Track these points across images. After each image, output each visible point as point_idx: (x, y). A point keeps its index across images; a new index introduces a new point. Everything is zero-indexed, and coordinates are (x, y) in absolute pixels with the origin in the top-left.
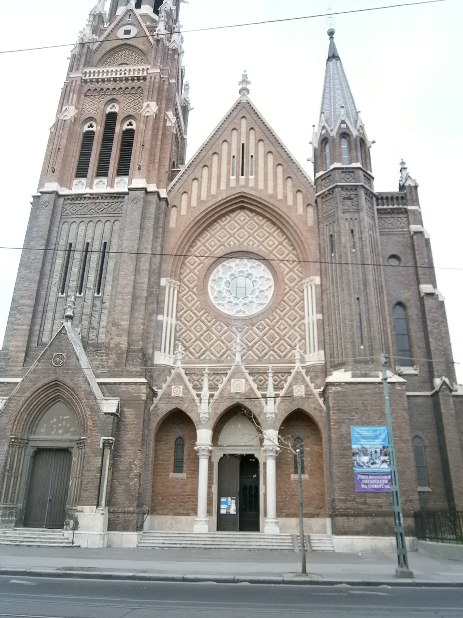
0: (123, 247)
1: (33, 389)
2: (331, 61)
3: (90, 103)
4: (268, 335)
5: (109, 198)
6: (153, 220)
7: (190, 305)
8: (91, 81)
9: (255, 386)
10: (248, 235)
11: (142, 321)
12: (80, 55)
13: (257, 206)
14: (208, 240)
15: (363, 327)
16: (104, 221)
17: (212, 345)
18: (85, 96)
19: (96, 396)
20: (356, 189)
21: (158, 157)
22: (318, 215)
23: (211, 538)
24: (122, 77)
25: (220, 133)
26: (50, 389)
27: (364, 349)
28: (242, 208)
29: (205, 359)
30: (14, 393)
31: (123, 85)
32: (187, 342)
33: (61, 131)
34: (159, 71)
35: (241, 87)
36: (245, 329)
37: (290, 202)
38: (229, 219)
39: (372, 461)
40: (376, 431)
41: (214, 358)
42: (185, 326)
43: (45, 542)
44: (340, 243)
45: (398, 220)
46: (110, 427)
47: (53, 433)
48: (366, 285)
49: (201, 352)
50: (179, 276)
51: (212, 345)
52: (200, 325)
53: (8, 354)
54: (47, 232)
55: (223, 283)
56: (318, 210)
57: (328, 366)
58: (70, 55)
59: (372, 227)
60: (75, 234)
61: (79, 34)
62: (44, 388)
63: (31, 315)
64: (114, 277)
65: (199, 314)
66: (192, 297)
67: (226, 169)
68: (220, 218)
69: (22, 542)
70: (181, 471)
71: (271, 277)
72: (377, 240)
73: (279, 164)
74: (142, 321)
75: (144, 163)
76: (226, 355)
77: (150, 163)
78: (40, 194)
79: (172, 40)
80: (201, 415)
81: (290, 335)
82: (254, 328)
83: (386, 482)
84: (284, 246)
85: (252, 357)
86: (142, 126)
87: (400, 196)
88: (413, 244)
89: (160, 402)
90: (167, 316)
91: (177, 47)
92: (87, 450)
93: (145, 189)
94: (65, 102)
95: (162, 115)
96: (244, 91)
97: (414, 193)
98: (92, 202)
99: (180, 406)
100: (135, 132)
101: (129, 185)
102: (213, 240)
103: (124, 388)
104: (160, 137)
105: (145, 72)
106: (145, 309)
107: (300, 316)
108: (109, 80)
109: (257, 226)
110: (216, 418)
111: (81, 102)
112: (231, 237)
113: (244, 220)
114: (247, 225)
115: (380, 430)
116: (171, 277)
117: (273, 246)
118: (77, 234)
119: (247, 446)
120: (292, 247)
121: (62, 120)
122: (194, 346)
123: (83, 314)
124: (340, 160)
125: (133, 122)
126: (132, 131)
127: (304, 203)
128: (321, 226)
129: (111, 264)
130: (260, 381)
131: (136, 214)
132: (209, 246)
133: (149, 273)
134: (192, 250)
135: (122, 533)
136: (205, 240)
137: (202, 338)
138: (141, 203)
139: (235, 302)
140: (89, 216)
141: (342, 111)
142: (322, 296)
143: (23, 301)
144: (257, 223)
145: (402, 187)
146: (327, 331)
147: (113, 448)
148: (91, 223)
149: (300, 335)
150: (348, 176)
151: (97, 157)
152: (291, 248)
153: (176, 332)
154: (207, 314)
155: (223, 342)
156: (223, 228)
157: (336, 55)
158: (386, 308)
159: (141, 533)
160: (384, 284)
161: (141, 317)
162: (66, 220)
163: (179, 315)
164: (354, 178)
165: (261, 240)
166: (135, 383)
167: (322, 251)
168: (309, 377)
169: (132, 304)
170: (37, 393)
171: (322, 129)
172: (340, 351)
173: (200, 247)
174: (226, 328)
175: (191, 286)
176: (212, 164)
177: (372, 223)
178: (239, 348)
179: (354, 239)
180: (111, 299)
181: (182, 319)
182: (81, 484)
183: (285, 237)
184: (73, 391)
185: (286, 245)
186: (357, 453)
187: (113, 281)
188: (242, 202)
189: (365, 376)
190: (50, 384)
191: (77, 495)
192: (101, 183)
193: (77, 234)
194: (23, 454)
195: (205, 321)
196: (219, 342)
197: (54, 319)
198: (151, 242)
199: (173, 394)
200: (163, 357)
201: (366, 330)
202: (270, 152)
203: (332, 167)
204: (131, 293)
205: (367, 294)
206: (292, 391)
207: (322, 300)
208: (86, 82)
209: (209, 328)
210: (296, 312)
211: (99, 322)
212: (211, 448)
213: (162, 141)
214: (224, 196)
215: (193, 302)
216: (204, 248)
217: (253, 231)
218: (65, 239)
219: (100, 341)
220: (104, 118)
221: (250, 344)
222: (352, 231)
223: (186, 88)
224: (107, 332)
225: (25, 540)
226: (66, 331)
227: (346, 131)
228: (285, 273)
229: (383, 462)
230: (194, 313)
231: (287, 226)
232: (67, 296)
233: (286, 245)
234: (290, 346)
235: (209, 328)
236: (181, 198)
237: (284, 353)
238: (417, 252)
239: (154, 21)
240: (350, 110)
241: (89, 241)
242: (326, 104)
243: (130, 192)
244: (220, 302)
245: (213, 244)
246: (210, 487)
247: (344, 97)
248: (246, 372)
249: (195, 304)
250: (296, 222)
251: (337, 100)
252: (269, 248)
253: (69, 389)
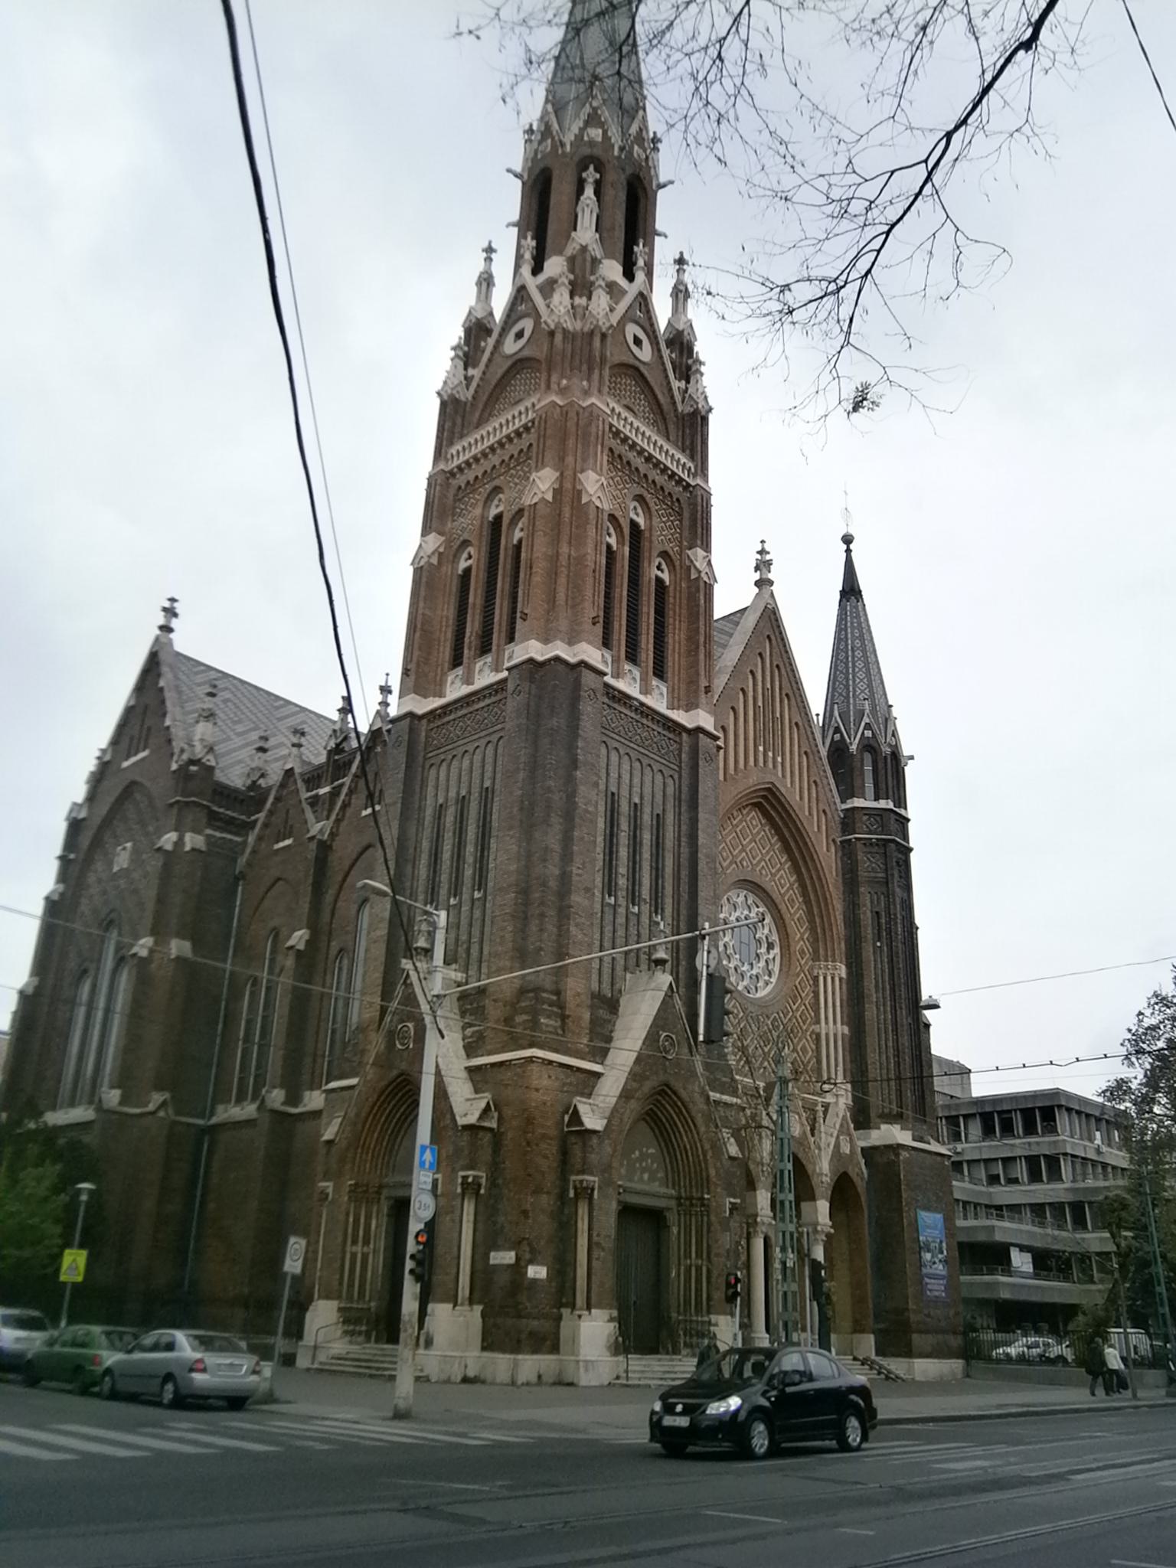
31: (661, 480)
118: (619, 776)
140: (635, 747)
188: (764, 797)
189: (921, 1140)
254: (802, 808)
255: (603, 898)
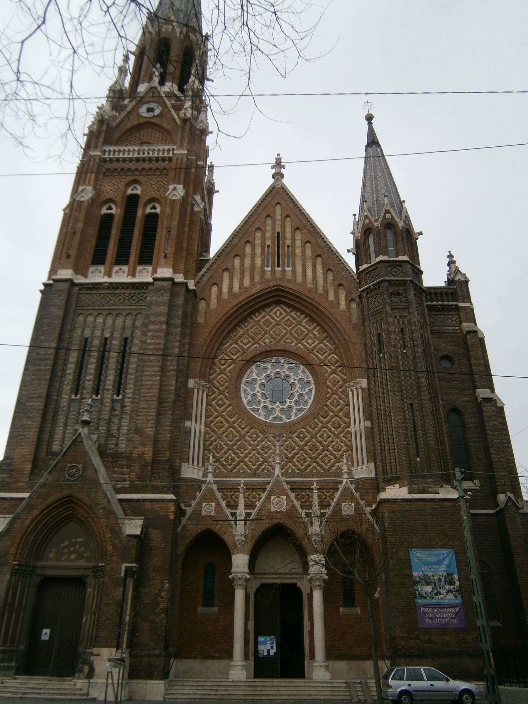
0: (148, 343)
1: (42, 506)
2: (371, 147)
3: (109, 184)
4: (309, 444)
5: (130, 288)
6: (180, 315)
7: (220, 410)
8: (111, 160)
9: (297, 504)
10: (285, 332)
11: (168, 428)
12: (99, 131)
13: (295, 301)
14: (240, 337)
15: (418, 437)
16: (124, 314)
17: (246, 456)
18: (104, 175)
19: (118, 515)
20: (404, 284)
21: (185, 244)
22: (363, 311)
23: (250, 686)
24: (145, 158)
25: (253, 220)
26: (62, 507)
27: (420, 462)
28: (278, 303)
29: (238, 472)
30: (19, 510)
31: (146, 165)
32: (218, 453)
33: (77, 213)
34: (185, 152)
35: (274, 171)
36: (284, 438)
37: (332, 297)
38: (264, 314)
39: (436, 591)
40: (439, 555)
41: (249, 471)
42: (216, 433)
43: (54, 694)
44: (390, 343)
45: (448, 318)
46: (133, 552)
47: (63, 559)
48: (420, 390)
49: (234, 464)
50: (208, 377)
51: (246, 456)
52: (233, 433)
53: (10, 465)
54: (60, 325)
55: (257, 386)
56: (362, 306)
57: (381, 481)
58: (87, 131)
59: (423, 326)
60: (91, 328)
61: (97, 110)
62: (55, 505)
63: (39, 419)
64: (136, 378)
65: (231, 421)
66: (223, 400)
67: (260, 260)
68: (253, 313)
69: (25, 693)
70: (212, 605)
71: (311, 379)
72: (429, 339)
73: (318, 256)
74: (168, 428)
75: (170, 251)
76: (263, 467)
77: (177, 251)
78: (51, 282)
79: (200, 120)
80: (237, 538)
81: (335, 445)
82: (294, 436)
83: (453, 615)
84: (325, 345)
85: (292, 469)
86: (168, 210)
87: (449, 292)
88: (466, 344)
89: (189, 522)
90: (196, 423)
91: (204, 127)
92: (106, 579)
93: (171, 280)
94: (82, 182)
95: (190, 199)
96: (278, 176)
97: (464, 289)
98: (111, 292)
99: (211, 527)
100: (160, 216)
101: (152, 275)
102: (246, 337)
103: (148, 506)
104: (187, 223)
105: (171, 153)
106: (173, 414)
107: (345, 423)
108: (131, 160)
109: (295, 323)
110: (254, 541)
111: (100, 182)
112: (265, 334)
113: (280, 315)
114: (283, 321)
115: (444, 554)
116: (199, 378)
117: (313, 345)
118: (94, 327)
119: (292, 574)
120: (334, 346)
121: (78, 201)
122: (225, 456)
123: (100, 419)
124: (386, 253)
125: (157, 205)
126: (156, 214)
127: (346, 297)
128: (367, 323)
129: (133, 362)
130: (303, 497)
131: (162, 307)
132: (241, 344)
133: (177, 373)
134: (223, 348)
135: (145, 681)
136: (237, 337)
137: (235, 448)
138: (168, 295)
139: (271, 407)
141: (386, 200)
142: (370, 400)
143: (30, 403)
144: (294, 319)
145: (450, 282)
146: (377, 441)
147: (136, 577)
148: (110, 316)
149: (346, 445)
150: (395, 270)
151: (117, 242)
152: (332, 348)
153: (205, 440)
154: (240, 420)
155: (259, 453)
156: (257, 323)
157: (376, 141)
158: (442, 415)
159: (168, 681)
160: (438, 388)
161: (168, 423)
162: (81, 312)
163: (208, 421)
164: (402, 272)
165: (299, 338)
166: (162, 500)
167: (369, 352)
168: (359, 493)
169: (158, 409)
170: (46, 511)
171: (365, 219)
172: (393, 464)
173: (232, 344)
174: (262, 436)
175: (222, 388)
176: (244, 253)
177: (422, 321)
178: (278, 458)
179: (403, 337)
180: (132, 402)
181: (212, 425)
182: (98, 621)
183: (325, 334)
184: (89, 508)
185: (327, 343)
186: (419, 582)
187: (135, 382)
188: (279, 295)
190: (63, 500)
191: (92, 634)
192: (121, 272)
193: (94, 327)
194: (27, 585)
195: (238, 428)
196: (254, 452)
197: (66, 425)
198: (179, 339)
199: (204, 513)
200: (191, 469)
201: (421, 439)
202: (308, 242)
203: (378, 260)
204: (157, 396)
205: (421, 400)
206: (340, 509)
207: (371, 406)
208: (105, 160)
209: (242, 437)
210: (340, 418)
211: (119, 429)
212: (248, 576)
213: (190, 227)
214: (259, 288)
215: (224, 407)
216: (236, 346)
217: (290, 328)
218: (79, 333)
219: (120, 451)
220: (125, 199)
221: (290, 455)
222: (402, 330)
223: (211, 169)
224: (129, 440)
225: (28, 691)
226: (83, 439)
227: (392, 221)
228: (326, 375)
229: (448, 592)
230: (226, 420)
231: (329, 323)
232: (82, 398)
233: (327, 343)
234: (335, 457)
235: (242, 437)
236: (210, 290)
237: (328, 466)
238: (471, 353)
239: (177, 98)
240: (393, 199)
241: (107, 336)
242: (368, 192)
243: (156, 282)
244: (254, 406)
245: (246, 341)
246: (246, 624)
247: (386, 185)
248: (288, 487)
249: (226, 408)
250: (339, 318)
251: (379, 188)
252: (308, 346)
253: (85, 506)
254: (314, 289)
255: (70, 397)
